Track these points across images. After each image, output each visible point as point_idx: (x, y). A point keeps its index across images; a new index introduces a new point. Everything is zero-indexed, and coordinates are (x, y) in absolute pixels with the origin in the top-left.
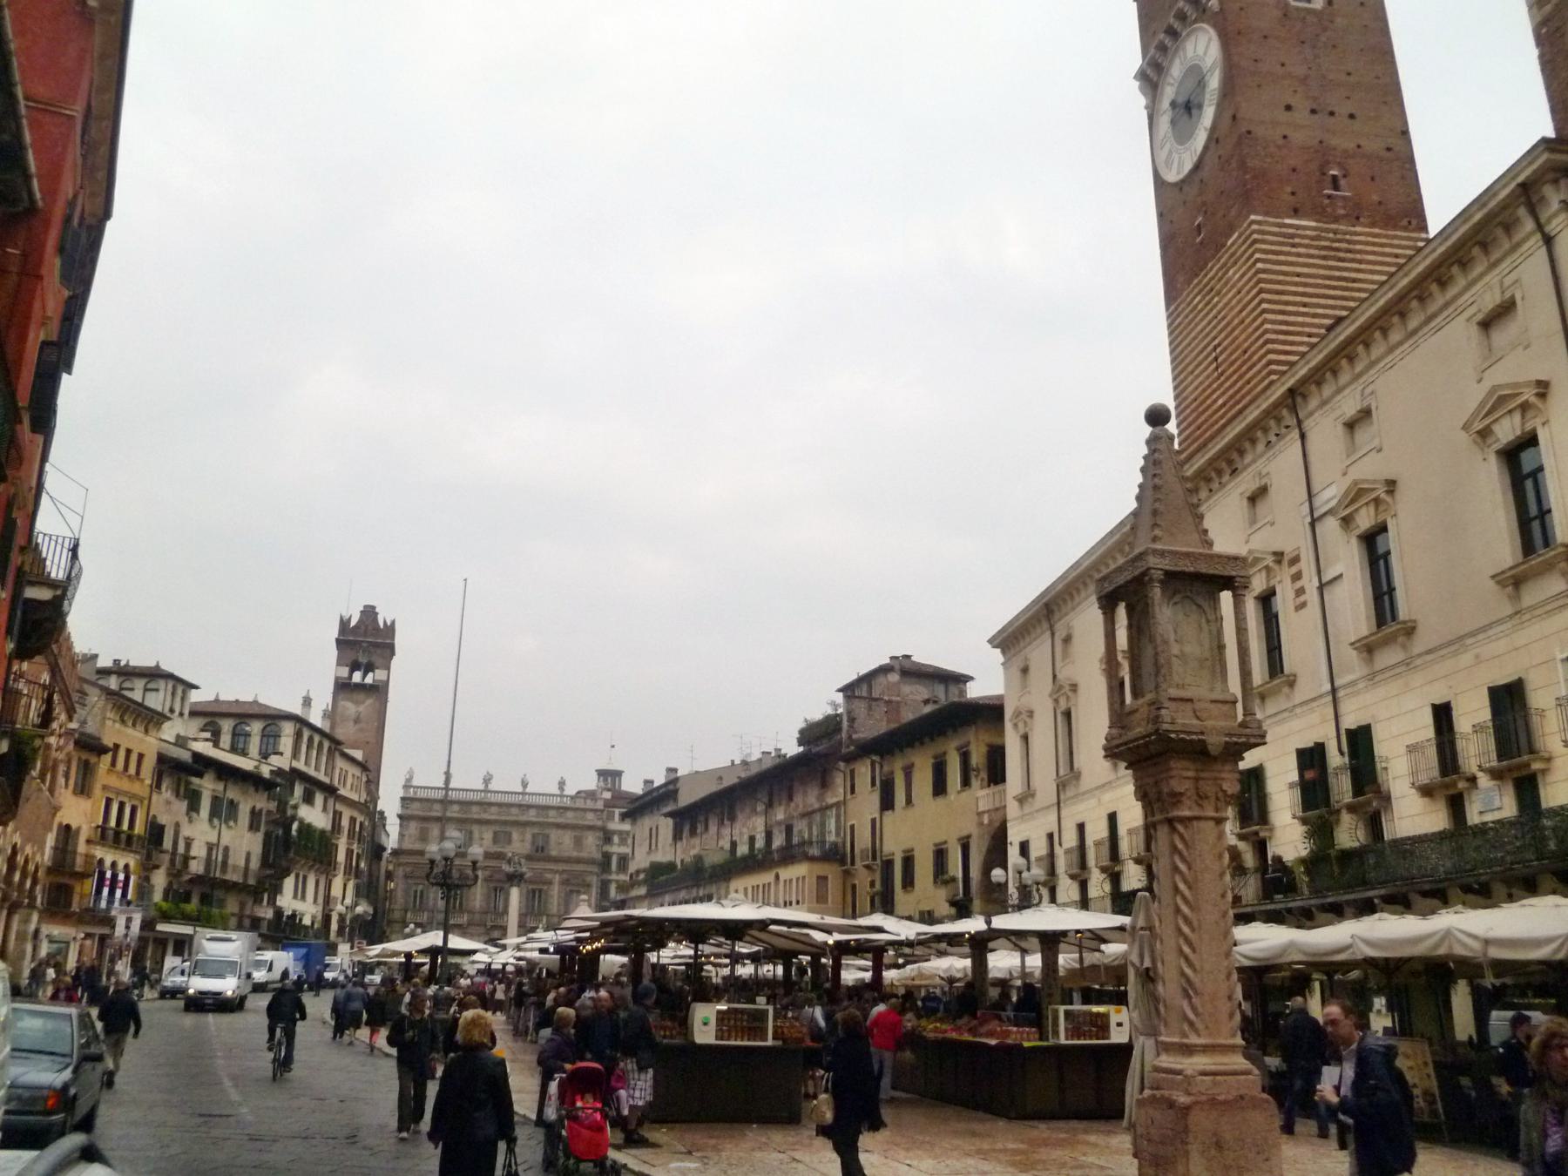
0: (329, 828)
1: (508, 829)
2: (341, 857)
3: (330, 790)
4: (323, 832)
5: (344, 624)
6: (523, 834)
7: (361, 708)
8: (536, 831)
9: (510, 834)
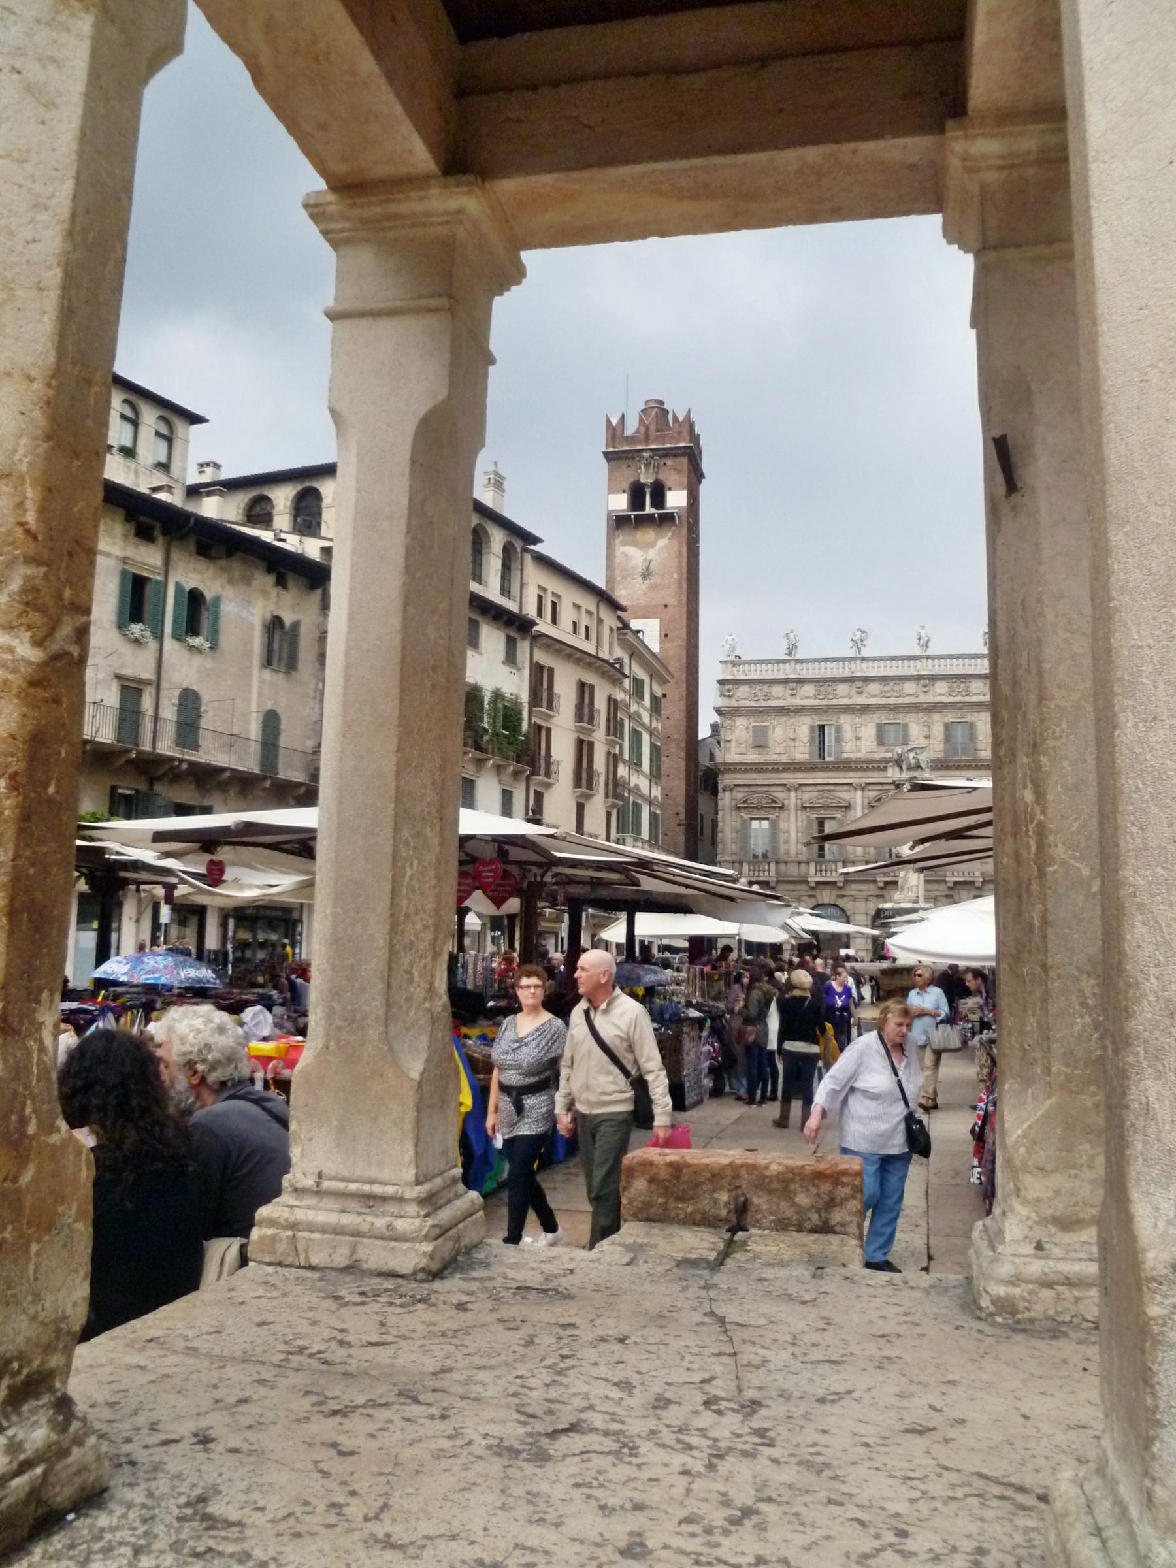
0: (525, 697)
1: (901, 719)
2: (562, 749)
3: (517, 626)
4: (497, 695)
5: (614, 433)
6: (928, 726)
7: (652, 554)
8: (950, 717)
9: (905, 727)
